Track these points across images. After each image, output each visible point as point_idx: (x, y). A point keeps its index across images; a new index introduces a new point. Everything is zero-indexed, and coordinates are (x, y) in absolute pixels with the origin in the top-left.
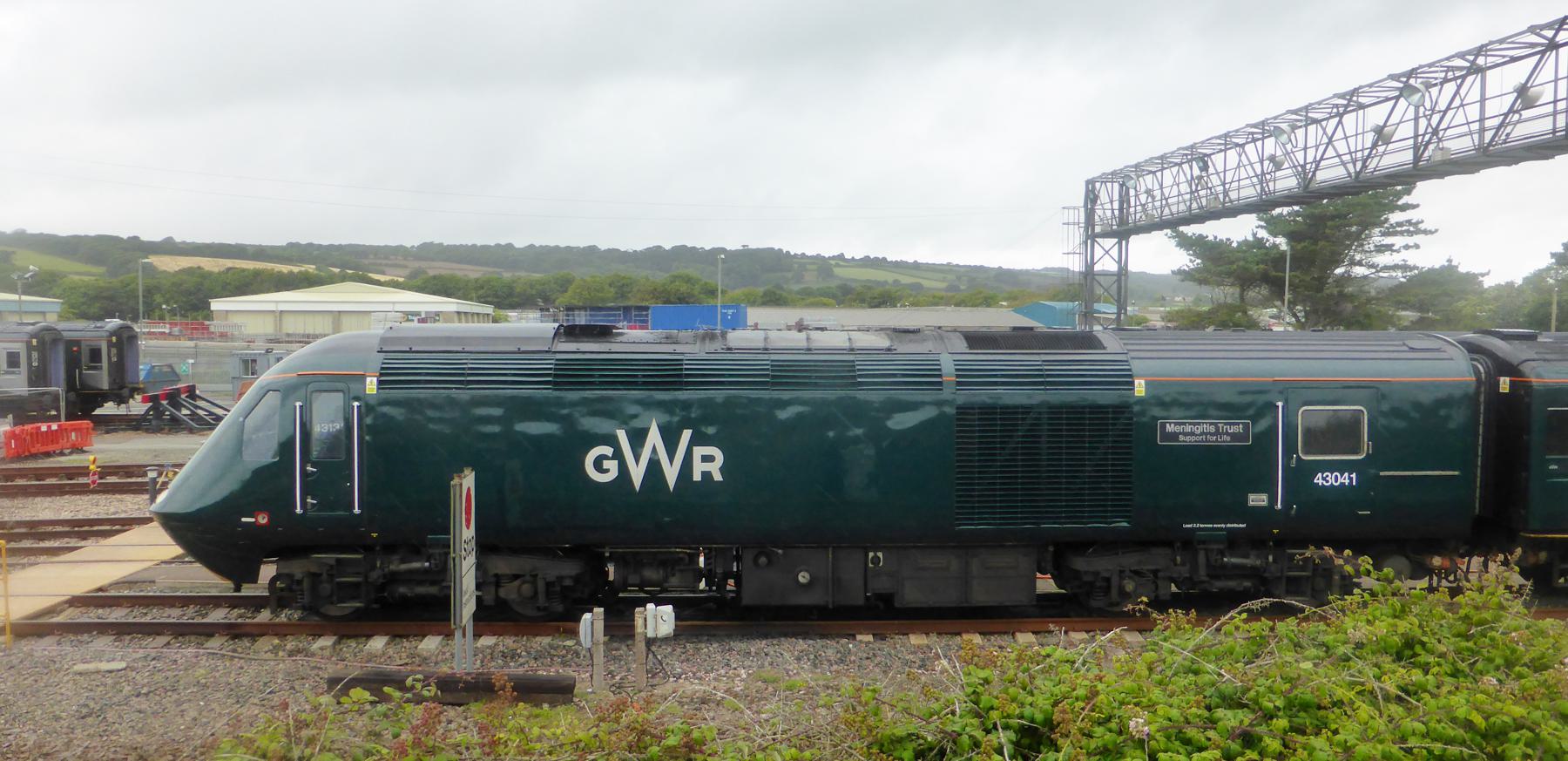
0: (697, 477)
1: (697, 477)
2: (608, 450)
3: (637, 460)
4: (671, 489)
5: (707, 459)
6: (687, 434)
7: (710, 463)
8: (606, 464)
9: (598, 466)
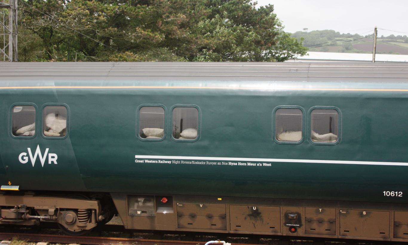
0: (50, 163)
1: (50, 163)
2: (25, 154)
3: (33, 156)
4: (43, 166)
5: (53, 157)
6: (47, 150)
7: (53, 158)
8: (25, 158)
9: (23, 158)
